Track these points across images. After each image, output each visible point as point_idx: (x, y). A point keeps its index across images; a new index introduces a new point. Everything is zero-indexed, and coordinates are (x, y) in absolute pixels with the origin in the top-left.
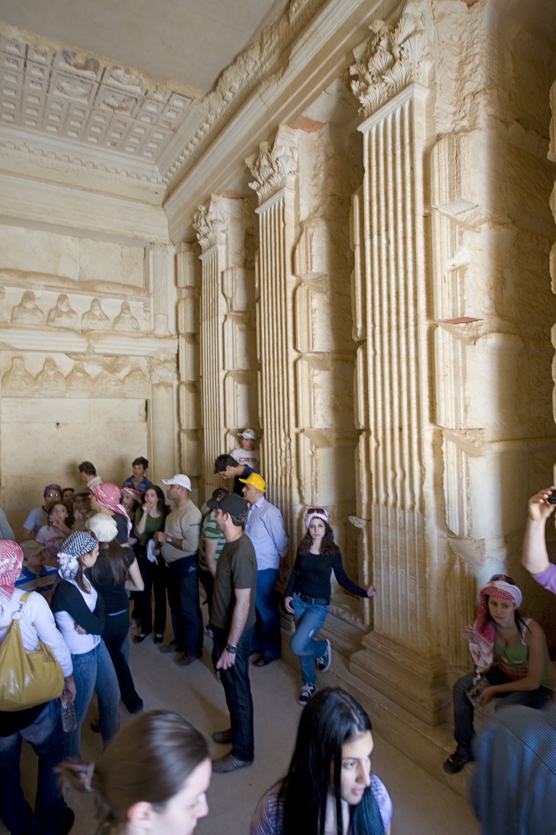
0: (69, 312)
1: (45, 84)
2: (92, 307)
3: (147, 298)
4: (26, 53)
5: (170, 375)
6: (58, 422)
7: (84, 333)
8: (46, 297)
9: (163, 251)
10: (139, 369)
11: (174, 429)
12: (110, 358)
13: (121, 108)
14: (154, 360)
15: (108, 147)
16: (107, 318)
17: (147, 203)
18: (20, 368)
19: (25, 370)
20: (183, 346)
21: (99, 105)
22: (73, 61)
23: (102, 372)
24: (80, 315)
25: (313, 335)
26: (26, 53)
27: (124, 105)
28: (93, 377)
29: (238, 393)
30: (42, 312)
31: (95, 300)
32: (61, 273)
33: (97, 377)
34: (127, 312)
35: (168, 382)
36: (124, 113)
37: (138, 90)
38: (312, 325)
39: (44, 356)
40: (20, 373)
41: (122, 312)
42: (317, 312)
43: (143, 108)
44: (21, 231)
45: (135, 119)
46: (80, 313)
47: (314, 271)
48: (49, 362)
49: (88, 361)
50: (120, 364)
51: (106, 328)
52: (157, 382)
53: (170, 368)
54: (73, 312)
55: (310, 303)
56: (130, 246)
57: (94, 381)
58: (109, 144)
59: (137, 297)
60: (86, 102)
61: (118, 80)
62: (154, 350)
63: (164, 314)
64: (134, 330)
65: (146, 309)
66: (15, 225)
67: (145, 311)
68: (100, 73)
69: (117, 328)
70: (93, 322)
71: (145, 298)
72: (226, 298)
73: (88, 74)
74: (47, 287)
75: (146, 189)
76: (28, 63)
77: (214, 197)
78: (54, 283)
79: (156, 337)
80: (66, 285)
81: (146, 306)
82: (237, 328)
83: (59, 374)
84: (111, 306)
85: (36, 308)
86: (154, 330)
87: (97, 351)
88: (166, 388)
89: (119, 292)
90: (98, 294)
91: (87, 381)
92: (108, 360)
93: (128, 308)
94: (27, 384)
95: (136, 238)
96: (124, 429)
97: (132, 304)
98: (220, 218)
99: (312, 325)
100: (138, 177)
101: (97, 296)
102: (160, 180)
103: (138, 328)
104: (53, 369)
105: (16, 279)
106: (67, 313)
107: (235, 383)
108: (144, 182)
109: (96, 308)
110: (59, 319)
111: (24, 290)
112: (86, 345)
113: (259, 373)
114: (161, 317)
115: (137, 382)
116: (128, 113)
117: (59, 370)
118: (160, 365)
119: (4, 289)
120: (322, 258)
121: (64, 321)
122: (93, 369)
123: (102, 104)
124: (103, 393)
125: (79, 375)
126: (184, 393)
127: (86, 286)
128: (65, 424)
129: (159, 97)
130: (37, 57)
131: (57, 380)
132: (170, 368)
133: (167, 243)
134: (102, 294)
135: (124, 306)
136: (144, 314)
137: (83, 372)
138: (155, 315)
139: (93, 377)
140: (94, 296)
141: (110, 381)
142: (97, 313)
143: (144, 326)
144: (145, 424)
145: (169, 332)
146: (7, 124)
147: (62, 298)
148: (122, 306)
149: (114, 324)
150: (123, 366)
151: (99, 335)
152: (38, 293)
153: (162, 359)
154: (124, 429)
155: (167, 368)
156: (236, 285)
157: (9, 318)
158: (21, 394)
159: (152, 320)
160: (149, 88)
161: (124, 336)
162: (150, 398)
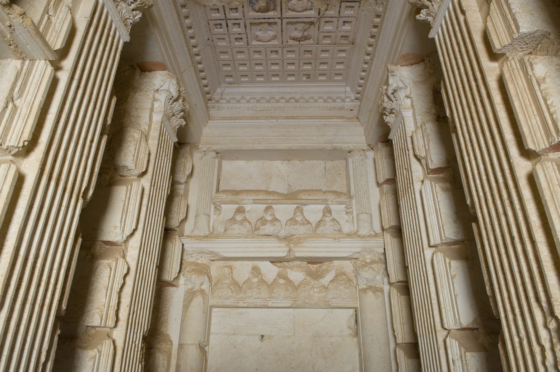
0: (272, 220)
1: (244, 36)
2: (295, 213)
3: (348, 200)
4: (225, 14)
5: (379, 278)
6: (263, 334)
7: (287, 239)
8: (254, 210)
9: (361, 155)
10: (344, 274)
11: (389, 344)
12: (315, 266)
13: (306, 38)
14: (359, 262)
15: (304, 81)
16: (309, 223)
17: (341, 117)
18: (228, 276)
19: (232, 278)
20: (389, 243)
21: (287, 42)
22: (257, 7)
23: (305, 279)
24: (284, 222)
25: (551, 115)
26: (225, 14)
27: (306, 34)
28: (296, 284)
29: (453, 274)
30: (250, 223)
31: (297, 207)
32: (270, 190)
33: (300, 284)
34: (328, 215)
35: (377, 286)
36: (307, 42)
37: (312, 13)
38: (545, 100)
39: (251, 264)
40: (227, 281)
41: (324, 216)
42: (548, 80)
43: (321, 30)
44: (241, 163)
45: (318, 44)
46: (284, 221)
47: (523, 30)
48: (256, 271)
49: (291, 268)
50: (324, 270)
51: (308, 232)
52: (365, 287)
53: (377, 270)
54: (276, 220)
55: (530, 73)
56: (332, 160)
57: (296, 288)
58: (304, 79)
59: (338, 200)
60: (277, 43)
61: (293, 10)
62: (358, 250)
63: (366, 213)
64: (337, 232)
65: (348, 211)
66: (237, 159)
67: (347, 213)
68: (279, 8)
69: (318, 232)
70: (295, 227)
71: (345, 200)
72: (419, 160)
73: (271, 14)
74: (255, 202)
75: (342, 108)
76: (229, 22)
77: (391, 67)
78: (261, 197)
79: (359, 236)
80: (271, 197)
81: (349, 207)
82: (438, 188)
83: (262, 281)
84: (313, 212)
85: (245, 219)
86: (358, 231)
87: (298, 255)
88: (374, 293)
89: (321, 197)
90: (300, 201)
91: (289, 288)
92: (313, 267)
93: (330, 212)
94: (232, 292)
95: (335, 149)
96: (332, 344)
97: (333, 207)
98: (401, 85)
99: (545, 100)
100: (334, 101)
101: (299, 203)
102: (353, 98)
103: (340, 230)
104: (256, 277)
105: (230, 197)
106: (271, 221)
107: (447, 260)
108: (339, 104)
109: (297, 214)
110: (264, 227)
111: (237, 206)
112: (287, 249)
113: (474, 225)
114: (363, 217)
115: (342, 287)
116: (311, 41)
117: (264, 278)
118: (365, 266)
119: (221, 207)
120: (532, 14)
121: (268, 229)
122: (296, 275)
123: (289, 40)
124: (307, 301)
125: (282, 281)
126: (396, 297)
127: (291, 196)
128: (270, 337)
129: (331, 13)
130: (233, 15)
131: (259, 287)
132: (377, 270)
133: (365, 148)
134: (303, 201)
135: (326, 210)
136: (346, 216)
137: (286, 278)
138: (357, 216)
139: (296, 284)
140: (296, 204)
141: (313, 287)
142: (299, 219)
143: (346, 229)
144: (355, 340)
145: (374, 231)
146: (230, 85)
147: (267, 209)
148: (323, 210)
149: (316, 228)
150: (328, 271)
151: (299, 239)
152: (248, 207)
153: (368, 261)
154: (332, 344)
155: (373, 269)
156: (428, 140)
157: (223, 231)
158: (228, 303)
159: (355, 221)
160: (320, 7)
161: (324, 237)
162: (358, 306)
